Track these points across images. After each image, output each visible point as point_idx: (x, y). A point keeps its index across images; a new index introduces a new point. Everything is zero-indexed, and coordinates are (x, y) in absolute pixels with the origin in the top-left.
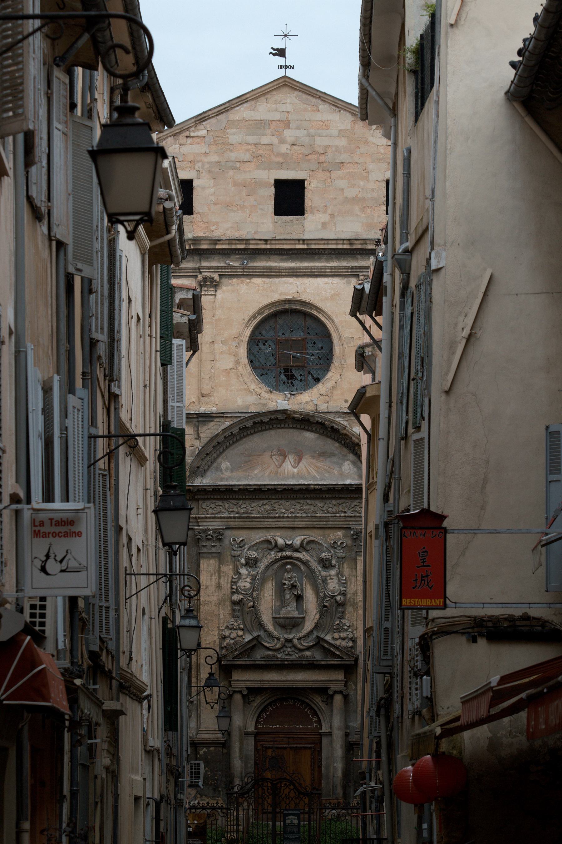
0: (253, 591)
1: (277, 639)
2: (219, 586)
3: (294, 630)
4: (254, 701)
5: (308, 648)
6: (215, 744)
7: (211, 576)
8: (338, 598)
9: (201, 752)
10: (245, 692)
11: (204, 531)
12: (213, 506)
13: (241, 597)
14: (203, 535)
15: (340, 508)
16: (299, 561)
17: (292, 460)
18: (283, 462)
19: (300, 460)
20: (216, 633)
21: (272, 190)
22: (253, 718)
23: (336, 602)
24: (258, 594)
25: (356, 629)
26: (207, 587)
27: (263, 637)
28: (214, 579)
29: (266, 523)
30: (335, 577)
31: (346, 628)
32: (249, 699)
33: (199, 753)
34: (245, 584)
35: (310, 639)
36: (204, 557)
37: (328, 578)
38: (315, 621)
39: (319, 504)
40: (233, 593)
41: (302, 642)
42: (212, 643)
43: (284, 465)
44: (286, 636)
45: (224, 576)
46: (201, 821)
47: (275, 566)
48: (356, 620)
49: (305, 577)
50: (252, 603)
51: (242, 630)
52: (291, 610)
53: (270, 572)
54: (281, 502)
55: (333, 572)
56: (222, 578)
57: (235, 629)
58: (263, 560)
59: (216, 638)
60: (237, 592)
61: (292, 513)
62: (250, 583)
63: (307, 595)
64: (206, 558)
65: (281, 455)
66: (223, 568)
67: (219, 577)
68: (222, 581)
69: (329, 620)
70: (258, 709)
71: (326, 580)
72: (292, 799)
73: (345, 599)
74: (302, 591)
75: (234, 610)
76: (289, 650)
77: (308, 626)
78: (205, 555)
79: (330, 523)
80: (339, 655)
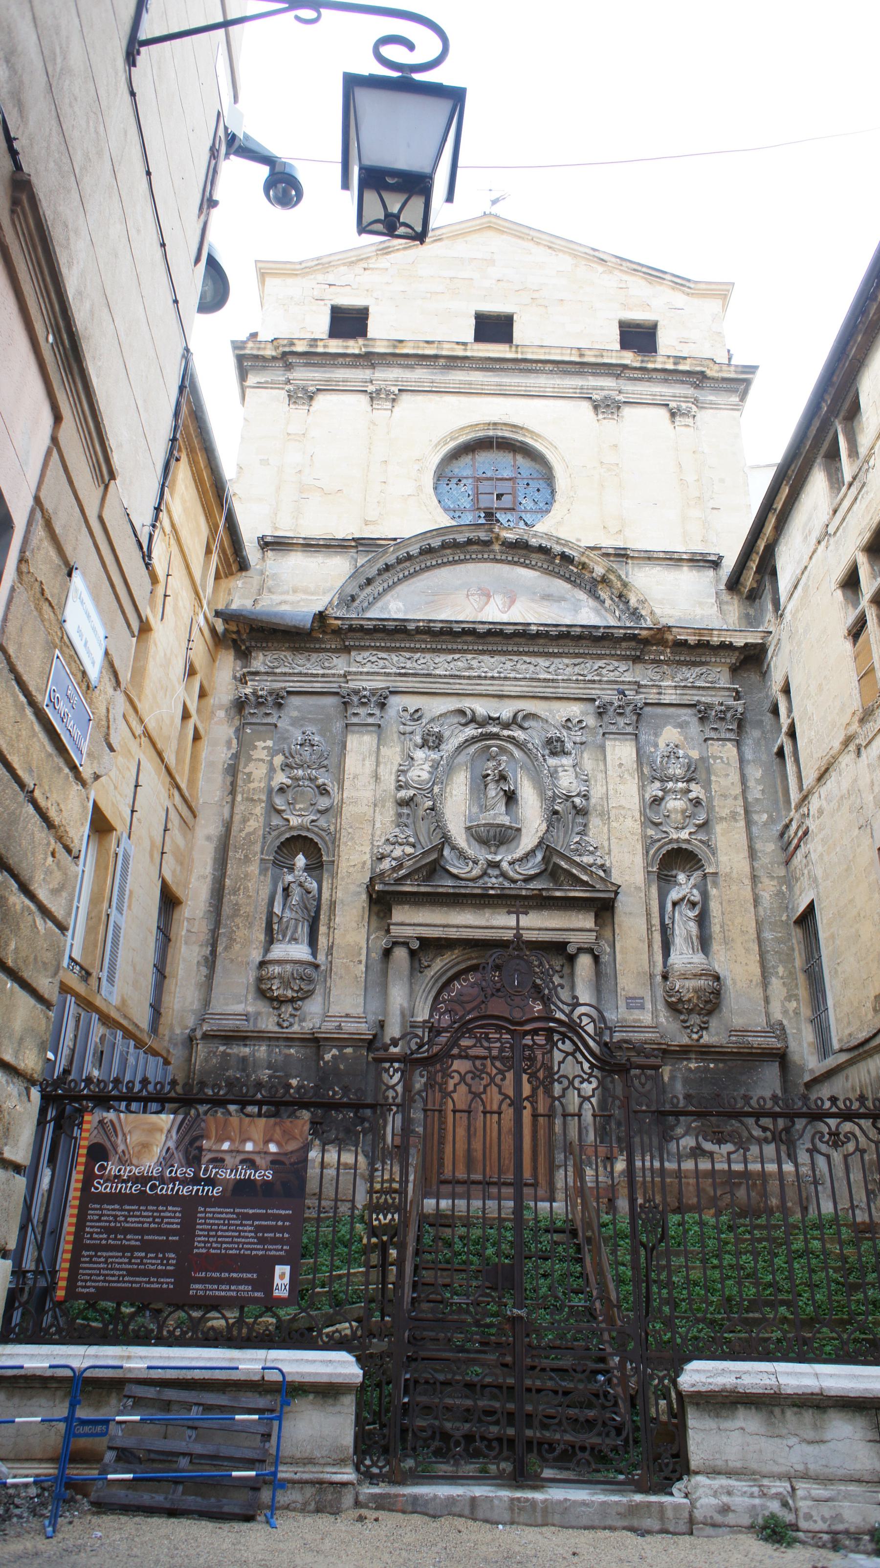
0: (433, 785)
1: (474, 862)
2: (376, 777)
3: (503, 849)
4: (429, 966)
5: (529, 879)
6: (355, 1041)
7: (364, 760)
8: (577, 800)
9: (328, 1057)
10: (415, 945)
11: (356, 692)
12: (374, 659)
13: (411, 792)
14: (355, 699)
15: (577, 670)
16: (511, 743)
17: (500, 603)
18: (487, 603)
19: (513, 602)
20: (367, 849)
21: (473, 321)
22: (429, 992)
23: (575, 807)
24: (441, 790)
25: (609, 853)
26: (356, 777)
27: (449, 858)
28: (370, 765)
29: (458, 686)
30: (572, 769)
31: (591, 849)
32: (420, 963)
33: (323, 1059)
34: (420, 772)
35: (530, 865)
36: (353, 732)
37: (560, 769)
38: (540, 834)
39: (543, 662)
40: (399, 788)
41: (517, 867)
42: (360, 866)
43: (487, 608)
44: (490, 857)
45: (385, 764)
46: (292, 1146)
47: (472, 749)
48: (609, 839)
49: (521, 767)
50: (431, 803)
51: (414, 846)
52: (499, 815)
53: (463, 758)
54: (481, 657)
55: (566, 761)
56: (382, 766)
57: (401, 844)
58: (451, 741)
59: (367, 857)
60: (407, 786)
61: (499, 672)
62: (429, 772)
63: (524, 796)
64: (358, 732)
65: (483, 594)
66: (383, 750)
67: (378, 764)
68: (381, 770)
69: (561, 834)
70: (436, 981)
71: (556, 772)
72: (571, 1083)
73: (588, 805)
74: (516, 788)
75: (400, 815)
76: (494, 880)
77: (528, 841)
78: (356, 728)
79: (561, 690)
80: (587, 882)
